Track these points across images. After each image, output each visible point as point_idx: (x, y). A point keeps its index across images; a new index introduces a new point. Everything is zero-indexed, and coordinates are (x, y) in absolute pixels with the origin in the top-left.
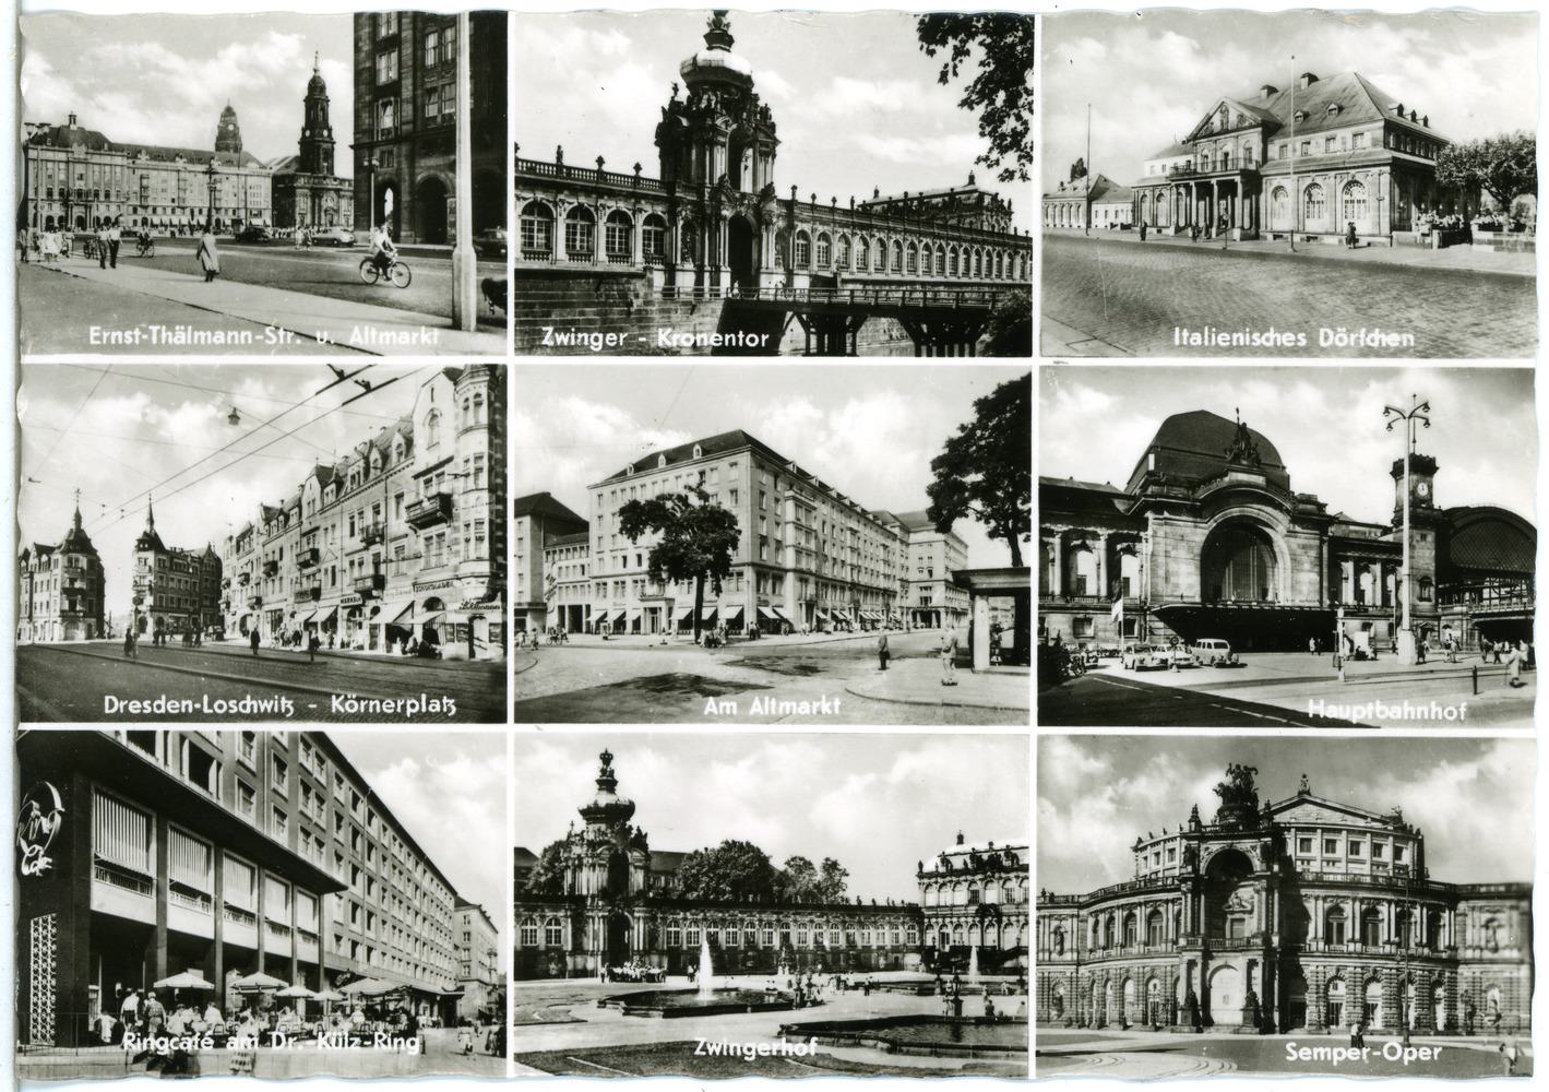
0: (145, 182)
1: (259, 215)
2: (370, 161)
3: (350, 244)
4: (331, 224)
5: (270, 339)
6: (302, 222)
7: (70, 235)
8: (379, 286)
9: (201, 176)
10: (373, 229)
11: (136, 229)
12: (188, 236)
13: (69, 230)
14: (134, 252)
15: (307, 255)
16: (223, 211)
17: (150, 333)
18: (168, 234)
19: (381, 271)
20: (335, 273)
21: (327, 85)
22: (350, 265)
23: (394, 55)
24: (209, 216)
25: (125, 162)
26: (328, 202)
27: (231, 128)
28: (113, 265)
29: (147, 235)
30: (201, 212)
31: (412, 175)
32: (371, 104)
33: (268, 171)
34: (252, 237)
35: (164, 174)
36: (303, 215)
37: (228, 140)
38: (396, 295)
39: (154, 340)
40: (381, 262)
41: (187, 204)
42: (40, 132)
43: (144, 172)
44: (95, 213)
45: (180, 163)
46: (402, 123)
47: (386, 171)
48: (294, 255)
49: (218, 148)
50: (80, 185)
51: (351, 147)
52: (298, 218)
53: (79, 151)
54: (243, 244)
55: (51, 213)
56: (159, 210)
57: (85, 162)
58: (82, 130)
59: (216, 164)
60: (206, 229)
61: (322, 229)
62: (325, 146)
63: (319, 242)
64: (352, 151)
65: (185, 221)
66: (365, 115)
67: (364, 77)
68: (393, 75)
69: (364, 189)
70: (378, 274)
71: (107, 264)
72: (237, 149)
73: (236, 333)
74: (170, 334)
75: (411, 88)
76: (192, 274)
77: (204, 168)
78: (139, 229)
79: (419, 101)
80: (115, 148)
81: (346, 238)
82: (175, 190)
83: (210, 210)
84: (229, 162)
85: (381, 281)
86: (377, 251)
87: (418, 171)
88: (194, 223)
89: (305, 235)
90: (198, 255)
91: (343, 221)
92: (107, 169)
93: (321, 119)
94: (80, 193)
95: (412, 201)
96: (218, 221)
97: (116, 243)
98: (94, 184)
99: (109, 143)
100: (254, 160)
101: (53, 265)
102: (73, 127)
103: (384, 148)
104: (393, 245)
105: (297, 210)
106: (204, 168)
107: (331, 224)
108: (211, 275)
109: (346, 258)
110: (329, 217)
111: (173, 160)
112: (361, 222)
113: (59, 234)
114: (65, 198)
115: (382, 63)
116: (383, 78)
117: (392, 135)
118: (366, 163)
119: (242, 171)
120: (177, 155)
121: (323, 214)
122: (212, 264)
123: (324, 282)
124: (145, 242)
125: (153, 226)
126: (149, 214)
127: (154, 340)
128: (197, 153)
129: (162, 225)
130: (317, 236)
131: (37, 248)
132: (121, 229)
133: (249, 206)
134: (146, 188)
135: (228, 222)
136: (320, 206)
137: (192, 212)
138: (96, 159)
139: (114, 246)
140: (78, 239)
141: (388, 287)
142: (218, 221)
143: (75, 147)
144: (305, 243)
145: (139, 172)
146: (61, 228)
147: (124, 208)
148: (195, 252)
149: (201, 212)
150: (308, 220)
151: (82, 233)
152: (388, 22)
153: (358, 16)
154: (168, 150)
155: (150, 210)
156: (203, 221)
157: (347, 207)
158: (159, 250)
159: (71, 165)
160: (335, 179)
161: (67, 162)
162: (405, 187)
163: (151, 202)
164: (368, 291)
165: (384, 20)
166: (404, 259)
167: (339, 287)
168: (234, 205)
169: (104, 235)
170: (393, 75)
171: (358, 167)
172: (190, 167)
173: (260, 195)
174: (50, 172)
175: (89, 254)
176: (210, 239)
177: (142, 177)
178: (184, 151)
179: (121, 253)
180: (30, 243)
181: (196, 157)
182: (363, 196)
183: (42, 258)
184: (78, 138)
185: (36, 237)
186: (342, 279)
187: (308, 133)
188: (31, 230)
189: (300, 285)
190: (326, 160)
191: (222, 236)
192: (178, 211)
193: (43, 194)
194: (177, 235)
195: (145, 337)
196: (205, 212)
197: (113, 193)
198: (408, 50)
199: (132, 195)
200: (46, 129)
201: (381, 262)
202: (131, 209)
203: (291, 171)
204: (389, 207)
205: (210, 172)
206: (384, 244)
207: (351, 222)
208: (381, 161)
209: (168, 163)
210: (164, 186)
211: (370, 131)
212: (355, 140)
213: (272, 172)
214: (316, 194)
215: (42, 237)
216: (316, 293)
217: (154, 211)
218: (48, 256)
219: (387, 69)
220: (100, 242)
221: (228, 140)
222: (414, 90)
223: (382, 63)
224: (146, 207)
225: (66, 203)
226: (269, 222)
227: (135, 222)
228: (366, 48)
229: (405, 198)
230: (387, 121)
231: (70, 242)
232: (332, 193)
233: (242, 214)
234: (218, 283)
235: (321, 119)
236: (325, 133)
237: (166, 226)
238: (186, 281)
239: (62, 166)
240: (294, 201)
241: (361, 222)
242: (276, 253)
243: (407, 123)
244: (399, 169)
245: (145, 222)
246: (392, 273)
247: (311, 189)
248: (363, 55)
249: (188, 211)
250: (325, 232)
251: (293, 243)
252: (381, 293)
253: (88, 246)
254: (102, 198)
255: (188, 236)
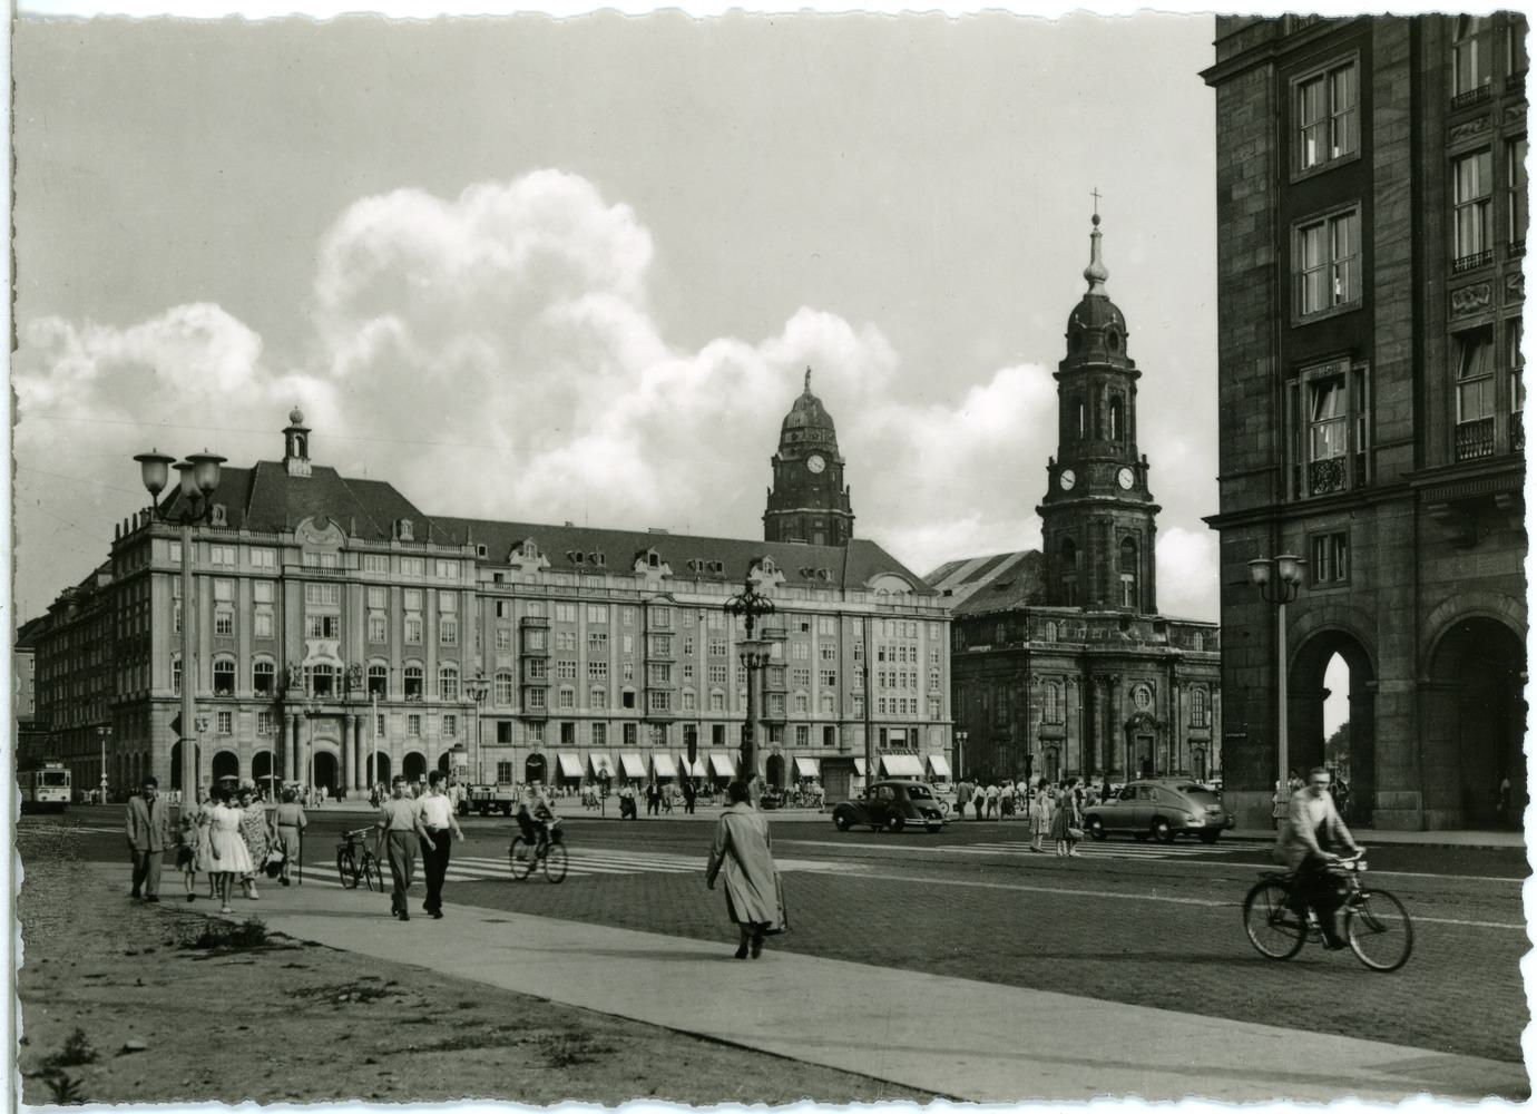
0: (535, 641)
2: (1274, 567)
6: (1053, 761)
7: (292, 811)
9: (716, 620)
11: (506, 793)
13: (288, 798)
18: (613, 809)
23: (1350, 228)
24: (747, 749)
26: (1138, 698)
28: (433, 907)
31: (1417, 609)
32: (1275, 383)
35: (598, 614)
36: (1054, 743)
42: (191, 485)
43: (534, 610)
45: (651, 580)
47: (1323, 602)
50: (322, 652)
52: (1038, 759)
55: (228, 745)
56: (583, 732)
57: (340, 580)
58: (325, 475)
59: (767, 583)
60: (737, 791)
62: (1124, 518)
65: (665, 766)
71: (415, 904)
72: (838, 529)
77: (726, 594)
78: (516, 792)
79: (1433, 376)
83: (748, 730)
84: (809, 577)
88: (699, 769)
89: (1063, 805)
91: (1185, 760)
96: (775, 764)
97: (443, 837)
98: (370, 648)
100: (892, 567)
103: (1320, 525)
106: (726, 594)
108: (754, 938)
113: (257, 809)
117: (1345, 485)
118: (1260, 574)
119: (854, 603)
120: (640, 554)
124: (536, 832)
129: (592, 777)
130: (1099, 807)
131: (184, 856)
132: (458, 791)
133: (876, 716)
135: (808, 768)
136: (1111, 714)
137: (691, 738)
138: (374, 569)
139: (438, 847)
140: (317, 825)
142: (775, 764)
144: (1061, 832)
145: (515, 611)
148: (701, 864)
155: (553, 731)
156: (725, 766)
159: (292, 588)
160: (1161, 625)
163: (555, 707)
166: (1390, 877)
171: (1233, 588)
172: (684, 593)
174: (224, 612)
176: (749, 820)
177: (524, 628)
179: (456, 871)
187: (1068, 480)
188: (164, 797)
190: (1128, 563)
191: (786, 814)
192: (644, 733)
194: (642, 809)
196: (733, 734)
197: (431, 677)
198: (1394, 209)
200: (209, 476)
202: (491, 729)
203: (1013, 602)
204: (1336, 714)
205: (750, 608)
207: (1215, 760)
208: (1310, 565)
209: (610, 582)
213: (952, 603)
216: (1100, 993)
217: (567, 731)
220: (390, 834)
223: (1312, 253)
224: (539, 723)
225: (277, 711)
226: (942, 766)
227: (505, 770)
229: (1392, 681)
231: (292, 833)
236: (1126, 478)
237: (606, 782)
239: (264, 592)
240: (1024, 698)
242: (963, 865)
245: (536, 770)
247: (1084, 660)
249: (676, 733)
251: (1024, 832)
254: (396, 695)
255: (679, 813)
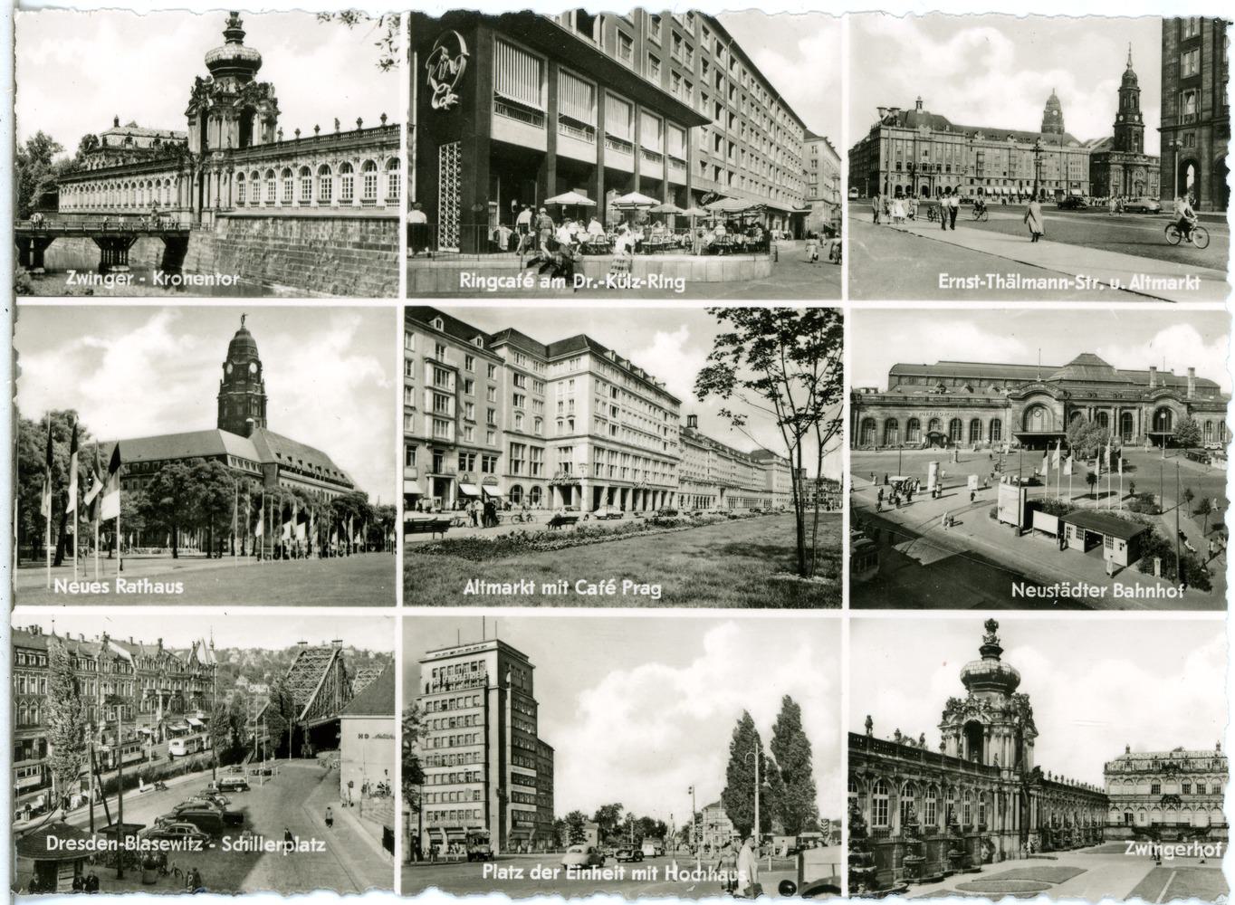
0: (981, 158)
1: (1078, 186)
2: (1175, 142)
3: (1156, 212)
4: (1141, 194)
5: (1080, 285)
7: (916, 201)
8: (1182, 246)
9: (1028, 153)
10: (1176, 198)
11: (972, 197)
12: (1017, 203)
13: (915, 198)
14: (971, 217)
15: (1120, 220)
16: (1047, 183)
17: (987, 280)
18: (1000, 202)
19: (1183, 234)
20: (1144, 235)
21: (1139, 78)
22: (1156, 229)
23: (1197, 53)
24: (1036, 187)
25: (964, 141)
26: (1138, 176)
27: (1055, 113)
28: (952, 227)
29: (982, 202)
30: (1028, 183)
32: (1176, 94)
33: (1086, 150)
34: (1072, 205)
35: (997, 151)
36: (1116, 187)
37: (1052, 120)
38: (1199, 255)
39: (990, 286)
40: (1183, 226)
41: (1017, 177)
42: (891, 115)
43: (981, 150)
44: (937, 183)
45: (1011, 142)
46: (1202, 111)
47: (1187, 152)
48: (1108, 220)
49: (1044, 130)
50: (924, 160)
51: (1159, 130)
53: (925, 131)
54: (1064, 210)
55: (900, 184)
56: (993, 182)
57: (930, 141)
58: (927, 114)
59: (1042, 144)
60: (1033, 198)
61: (1133, 198)
63: (1129, 210)
64: (1159, 134)
65: (1014, 191)
66: (1171, 103)
67: (1171, 72)
68: (1195, 69)
69: (1170, 165)
70: (1181, 237)
71: (948, 226)
72: (1060, 131)
73: (1055, 280)
74: (1003, 280)
75: (1210, 80)
76: (1020, 235)
77: (1031, 146)
78: (975, 198)
80: (956, 130)
81: (1153, 206)
82: (1006, 165)
83: (1036, 182)
84: (1053, 142)
85: (1183, 242)
86: (1180, 217)
87: (1216, 150)
88: (1023, 192)
90: (1026, 220)
91: (1151, 192)
92: (949, 146)
93: (1132, 106)
94: (925, 168)
95: (1211, 176)
96: (1043, 191)
99: (950, 125)
100: (1073, 140)
101: (901, 226)
102: (919, 111)
103: (1187, 131)
104: (1193, 213)
105: (1111, 182)
106: (1031, 146)
107: (1141, 194)
108: (1036, 236)
109: (1154, 224)
110: (1139, 188)
111: (1005, 140)
112: (1166, 192)
113: (907, 201)
114: (912, 170)
115: (1186, 60)
116: (1186, 73)
118: (1171, 144)
119: (1064, 149)
121: (1133, 186)
122: (1038, 228)
123: (1134, 243)
124: (980, 208)
125: (987, 194)
126: (983, 185)
127: (990, 286)
128: (1025, 133)
129: (995, 194)
130: (1128, 204)
131: (887, 212)
134: (982, 163)
135: (1052, 192)
136: (1131, 180)
138: (939, 138)
139: (954, 212)
140: (922, 205)
141: (1190, 248)
142: (1043, 191)
143: (921, 128)
144: (1117, 210)
145: (975, 150)
146: (908, 195)
147: (962, 180)
148: (1023, 217)
149: (1028, 183)
150: (1121, 191)
151: (926, 200)
152: (1192, 26)
153: (1165, 22)
154: (1002, 132)
155: (985, 181)
156: (1030, 191)
157: (1154, 180)
158: (992, 215)
160: (1145, 157)
161: (914, 141)
162: (1205, 163)
163: (985, 175)
164: (1172, 251)
165: (1188, 24)
166: (1203, 224)
167: (1147, 247)
168: (1056, 178)
169: (945, 202)
170: (1195, 69)
171: (1164, 147)
172: (1020, 146)
173: (1078, 169)
174: (899, 149)
175: (932, 217)
176: (1036, 206)
177: (978, 154)
178: (1014, 132)
179: (959, 217)
180: (881, 208)
181: (1025, 138)
182: (1169, 171)
183: (892, 221)
184: (924, 120)
185: (886, 203)
186: (1150, 241)
187: (1121, 118)
188: (882, 197)
189: (1113, 245)
190: (1136, 140)
191: (1046, 204)
192: (1009, 182)
193: (893, 167)
195: (983, 283)
196: (1032, 183)
197: (953, 167)
198: (1208, 49)
199: (969, 169)
200: (897, 113)
201: (1183, 226)
202: (968, 181)
203: (1106, 150)
204: (1190, 181)
205: (1037, 150)
206: (1186, 212)
207: (1158, 193)
208: (1184, 142)
209: (1000, 143)
210: (997, 162)
211: (1175, 117)
212: (1162, 124)
213: (1090, 150)
214: (1128, 168)
215: (892, 203)
216: (1127, 253)
217: (988, 182)
218: (897, 219)
219: (1190, 64)
220: (941, 207)
221: (1052, 120)
222: (1214, 83)
223: (1186, 60)
224: (981, 179)
225: (912, 175)
226: (1087, 193)
227: (972, 192)
228: (1172, 46)
229: (1205, 173)
230: (1190, 109)
231: (916, 207)
232: (1142, 169)
233: (1064, 186)
234: (1042, 243)
235: (1132, 106)
236: (1137, 118)
237: (998, 195)
238: (1015, 241)
239: (910, 144)
241: (1166, 192)
243: (1206, 110)
244: (1200, 148)
245: (980, 192)
246: (1193, 235)
248: (1169, 53)
249: (1017, 183)
250: (1135, 201)
251: (1107, 210)
252: (1183, 252)
253: (932, 212)
254: (944, 171)
255: (1017, 203)
